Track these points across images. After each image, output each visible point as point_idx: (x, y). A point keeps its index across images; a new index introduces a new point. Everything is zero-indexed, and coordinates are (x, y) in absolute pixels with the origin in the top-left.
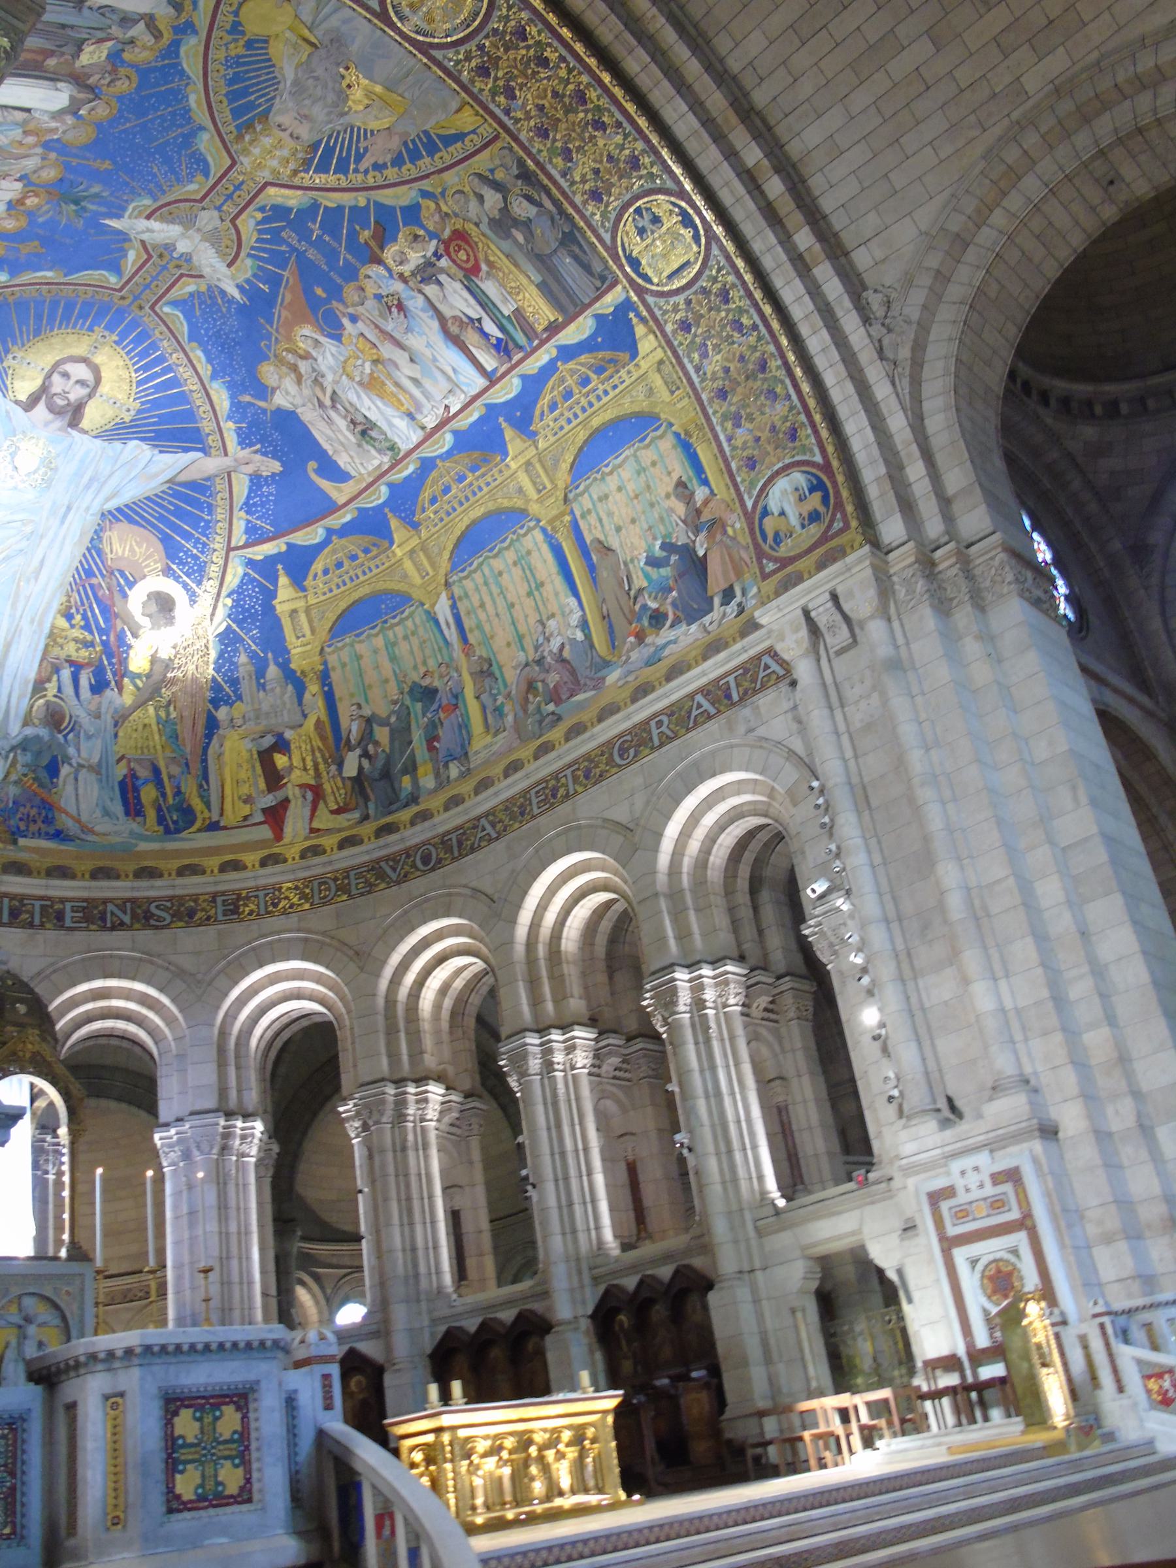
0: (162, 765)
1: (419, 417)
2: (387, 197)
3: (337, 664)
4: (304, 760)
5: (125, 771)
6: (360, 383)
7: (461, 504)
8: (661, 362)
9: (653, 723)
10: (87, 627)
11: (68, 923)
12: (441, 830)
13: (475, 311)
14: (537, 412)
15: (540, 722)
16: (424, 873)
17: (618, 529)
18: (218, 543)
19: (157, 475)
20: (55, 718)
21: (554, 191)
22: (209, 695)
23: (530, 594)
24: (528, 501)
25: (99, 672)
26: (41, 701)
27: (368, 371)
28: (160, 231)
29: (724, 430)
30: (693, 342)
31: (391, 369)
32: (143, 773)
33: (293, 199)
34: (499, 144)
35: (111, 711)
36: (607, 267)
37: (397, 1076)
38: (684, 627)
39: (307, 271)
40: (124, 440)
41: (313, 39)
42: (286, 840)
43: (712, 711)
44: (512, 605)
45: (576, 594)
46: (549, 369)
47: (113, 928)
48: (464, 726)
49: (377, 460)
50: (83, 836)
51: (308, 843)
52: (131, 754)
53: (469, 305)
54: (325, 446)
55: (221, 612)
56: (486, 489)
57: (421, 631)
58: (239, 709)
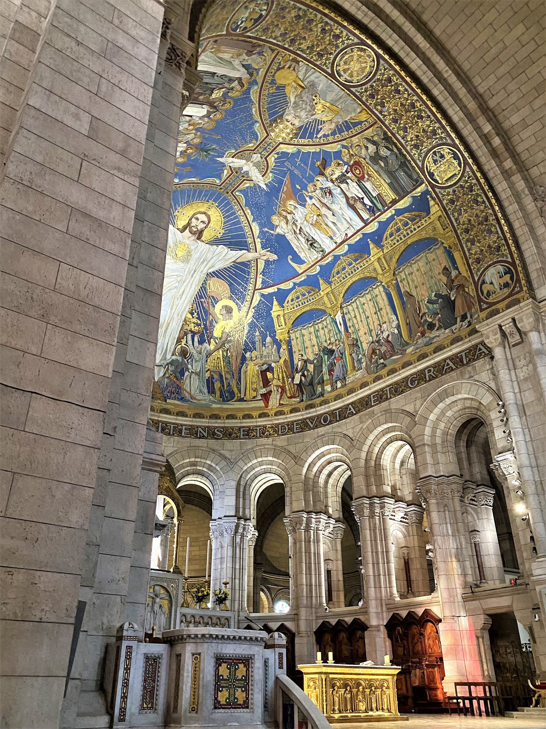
1: (334, 238)
2: (327, 148)
3: (294, 338)
6: (312, 224)
7: (349, 275)
8: (440, 217)
9: (426, 371)
10: (198, 318)
11: (183, 434)
12: (332, 408)
13: (361, 195)
14: (385, 237)
15: (377, 367)
16: (324, 426)
17: (416, 287)
19: (229, 259)
20: (184, 353)
21: (398, 144)
22: (243, 347)
23: (375, 313)
24: (378, 274)
26: (180, 346)
27: (315, 219)
28: (237, 163)
29: (467, 246)
30: (455, 208)
31: (325, 218)
32: (216, 377)
33: (291, 150)
34: (376, 126)
36: (419, 176)
37: (308, 510)
38: (443, 330)
39: (294, 179)
40: (217, 245)
41: (303, 85)
43: (454, 367)
44: (368, 317)
45: (396, 314)
46: (391, 218)
47: (200, 438)
48: (344, 366)
49: (315, 256)
52: (212, 369)
53: (359, 192)
54: (296, 249)
55: (251, 314)
56: (360, 269)
57: (329, 326)
58: (254, 353)
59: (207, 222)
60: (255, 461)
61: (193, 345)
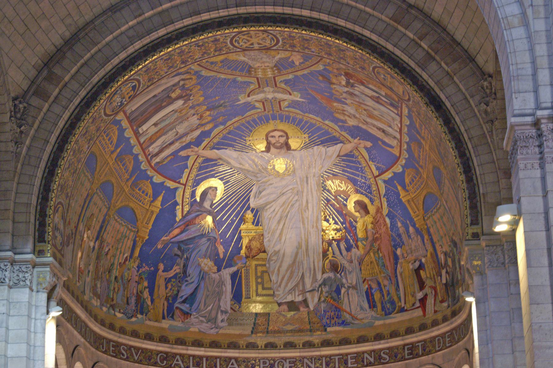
0: (380, 281)
4: (430, 273)
5: (367, 286)
10: (336, 223)
18: (370, 176)
20: (335, 267)
22: (393, 243)
25: (347, 241)
26: (328, 261)
32: (374, 286)
35: (356, 258)
42: (427, 317)
47: (367, 366)
50: (353, 322)
51: (434, 317)
59: (285, 135)
61: (341, 253)
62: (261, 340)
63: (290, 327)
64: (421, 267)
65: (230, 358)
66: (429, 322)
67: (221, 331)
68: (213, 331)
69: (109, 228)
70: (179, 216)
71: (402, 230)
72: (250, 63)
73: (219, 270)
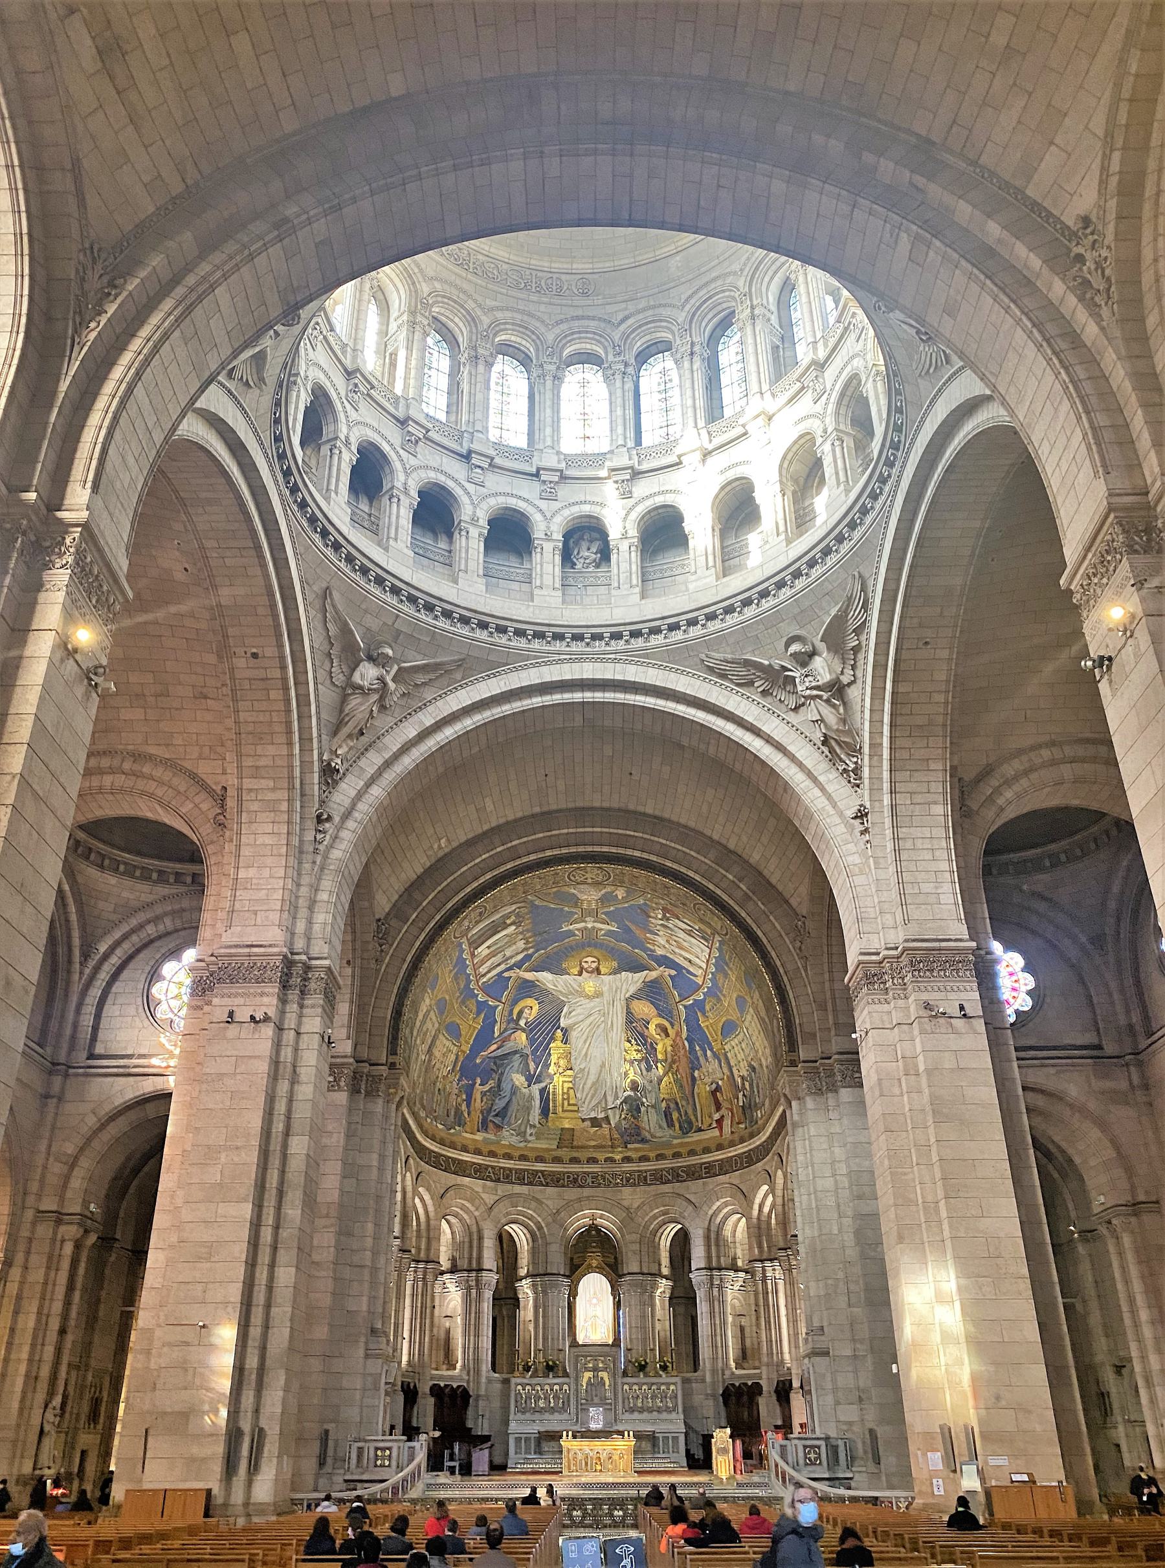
25: (648, 1062)
32: (672, 1106)
52: (666, 1096)
60: (718, 1204)
62: (564, 1153)
63: (593, 1143)
64: (718, 1089)
65: (537, 1171)
66: (726, 1143)
67: (530, 1145)
68: (522, 1145)
69: (438, 1042)
70: (496, 1035)
71: (699, 1053)
72: (579, 896)
73: (529, 1086)
